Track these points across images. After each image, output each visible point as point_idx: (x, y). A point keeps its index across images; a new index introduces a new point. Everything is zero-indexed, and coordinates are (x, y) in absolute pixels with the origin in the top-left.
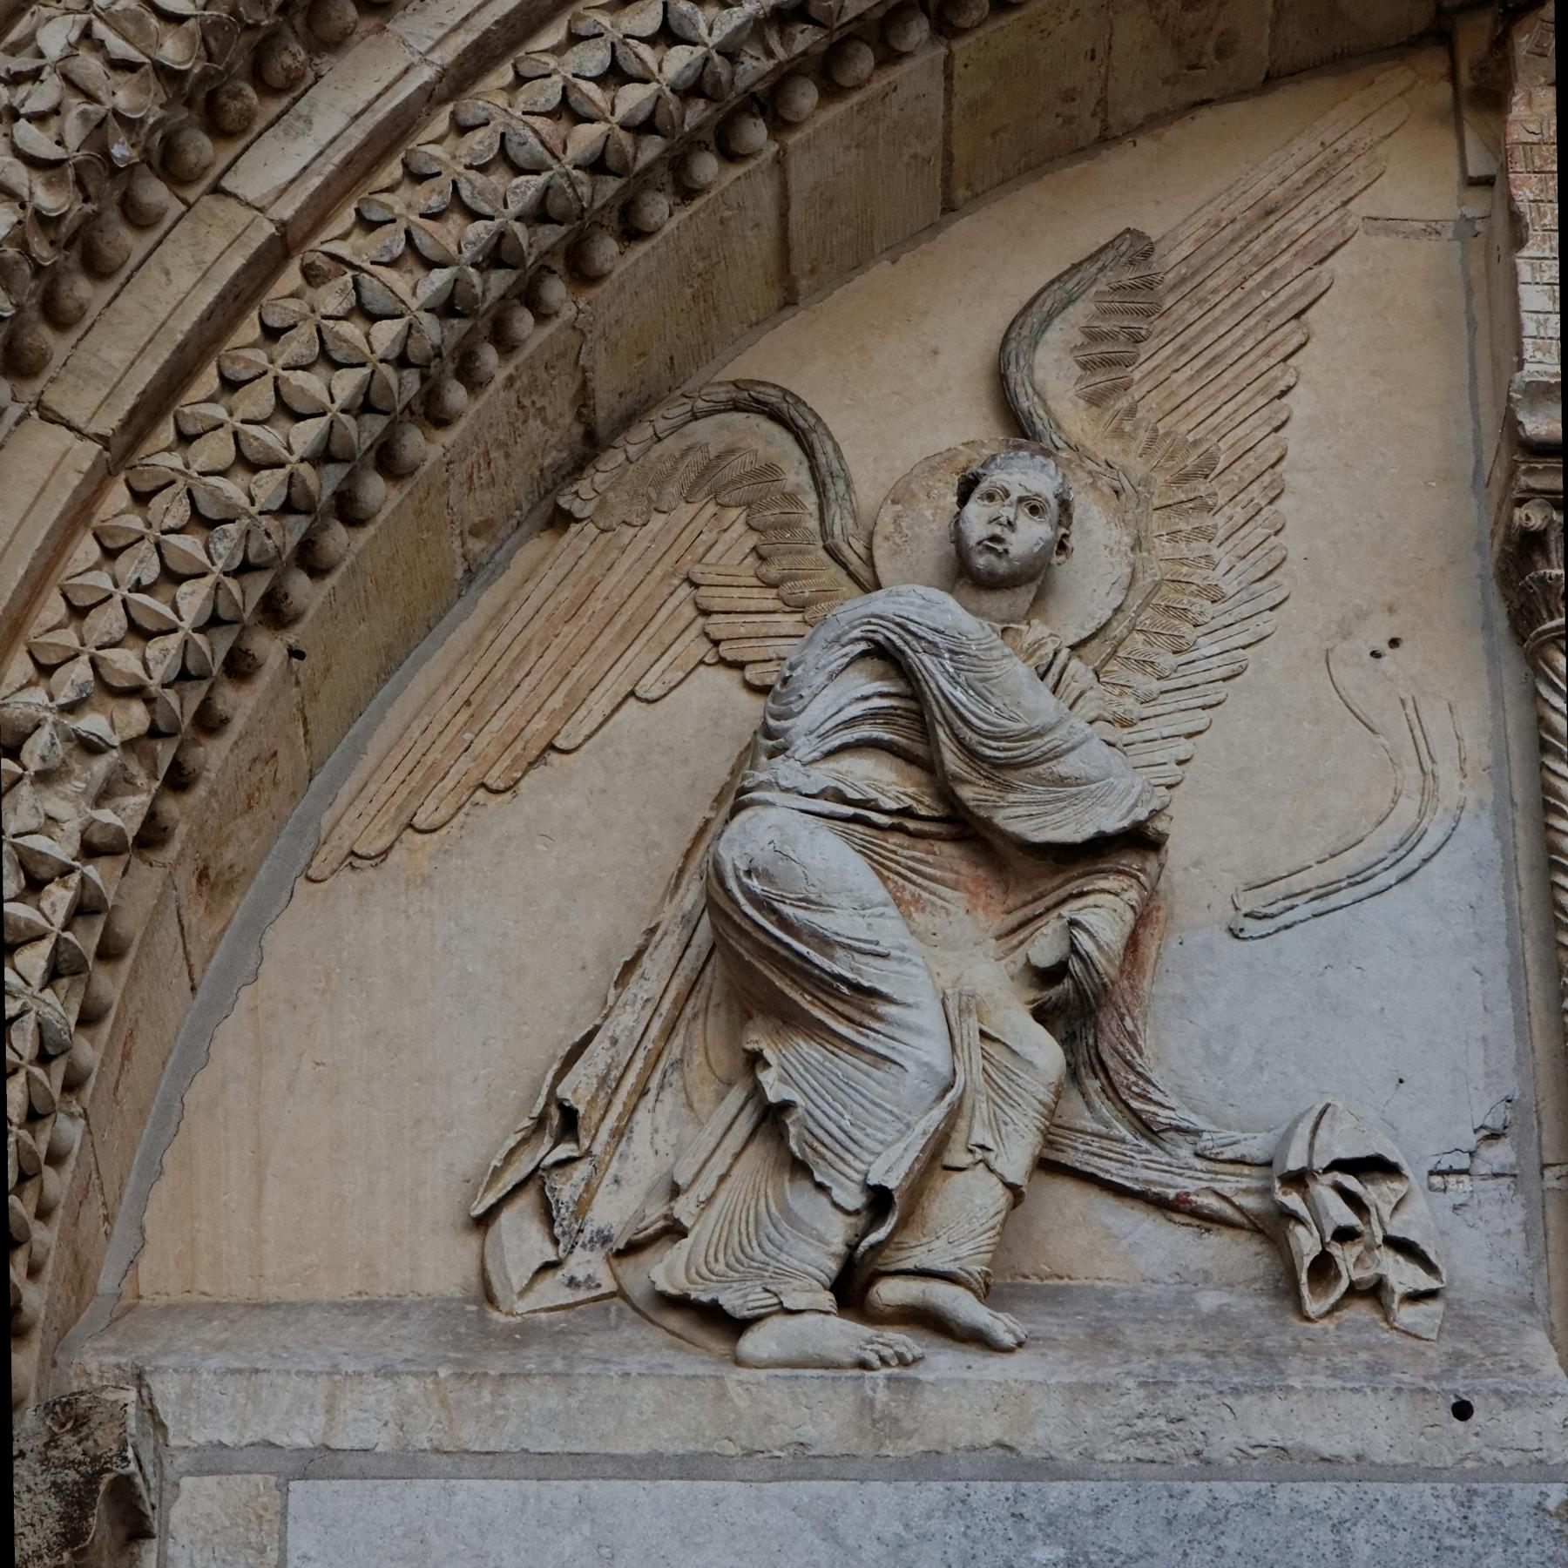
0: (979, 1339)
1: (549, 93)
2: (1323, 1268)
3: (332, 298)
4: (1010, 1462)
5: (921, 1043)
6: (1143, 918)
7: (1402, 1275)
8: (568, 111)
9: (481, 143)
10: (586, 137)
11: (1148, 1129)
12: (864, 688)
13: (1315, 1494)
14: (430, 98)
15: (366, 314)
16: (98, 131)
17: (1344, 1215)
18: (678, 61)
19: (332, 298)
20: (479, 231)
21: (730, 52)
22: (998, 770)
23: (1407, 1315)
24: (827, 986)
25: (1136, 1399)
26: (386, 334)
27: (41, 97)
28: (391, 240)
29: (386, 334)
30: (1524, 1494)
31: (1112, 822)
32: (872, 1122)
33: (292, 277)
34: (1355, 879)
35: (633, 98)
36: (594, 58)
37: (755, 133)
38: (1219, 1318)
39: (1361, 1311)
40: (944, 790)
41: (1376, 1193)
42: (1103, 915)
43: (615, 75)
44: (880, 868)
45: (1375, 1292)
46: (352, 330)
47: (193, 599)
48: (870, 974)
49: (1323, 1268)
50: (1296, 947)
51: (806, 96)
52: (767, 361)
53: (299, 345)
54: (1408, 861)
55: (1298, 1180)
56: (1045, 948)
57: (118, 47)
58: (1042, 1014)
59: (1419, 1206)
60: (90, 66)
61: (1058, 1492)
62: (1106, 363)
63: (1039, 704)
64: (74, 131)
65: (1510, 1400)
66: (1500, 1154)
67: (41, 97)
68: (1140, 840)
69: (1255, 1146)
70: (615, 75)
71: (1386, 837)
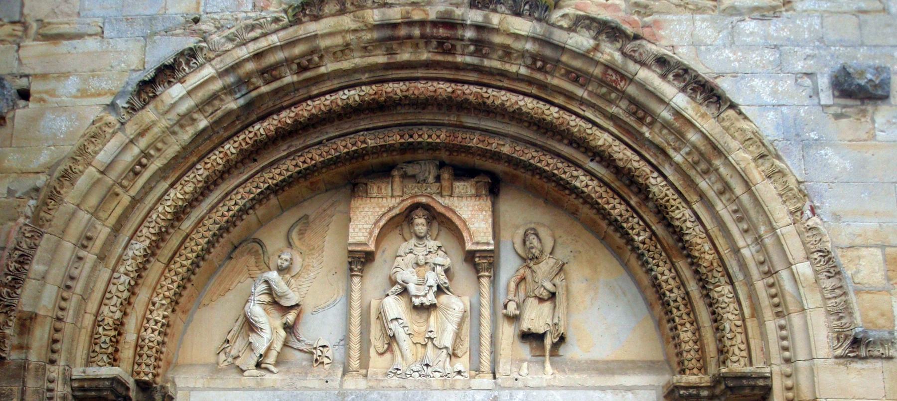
0: (272, 372)
1: (220, 214)
2: (317, 360)
3: (193, 243)
4: (274, 389)
5: (267, 335)
6: (298, 315)
7: (326, 361)
8: (223, 215)
9: (211, 221)
10: (225, 219)
11: (299, 341)
12: (264, 286)
13: (308, 392)
14: (206, 214)
15: (197, 245)
16: (160, 228)
17: (320, 353)
18: (237, 207)
19: (193, 243)
20: (211, 233)
21: (244, 205)
22: (279, 297)
23: (326, 367)
24: (257, 328)
25: (289, 381)
26: (200, 247)
27: (152, 225)
28: (200, 235)
29: (200, 247)
30: (333, 392)
31: (293, 304)
32: (261, 343)
33: (188, 240)
34: (328, 306)
35: (231, 213)
36: (226, 208)
37: (251, 211)
38: (304, 367)
39: (321, 366)
40: (274, 298)
41: (325, 350)
42: (291, 317)
43: (229, 210)
44: (264, 310)
45: (323, 363)
46: (195, 248)
47: (175, 285)
48: (262, 326)
49: (317, 360)
50: (319, 315)
51: (257, 206)
52: (256, 236)
53: (189, 250)
54: (334, 303)
55: (315, 348)
56: (284, 321)
57: (162, 217)
58: (284, 329)
59: (330, 351)
60: (159, 220)
61: (279, 393)
62: (301, 233)
63: (285, 288)
64: (157, 229)
65: (332, 381)
66: (342, 343)
67: (152, 225)
68: (297, 305)
69: (311, 342)
70: (229, 210)
71: (333, 299)
